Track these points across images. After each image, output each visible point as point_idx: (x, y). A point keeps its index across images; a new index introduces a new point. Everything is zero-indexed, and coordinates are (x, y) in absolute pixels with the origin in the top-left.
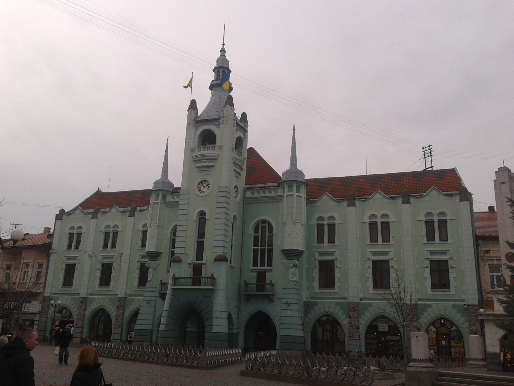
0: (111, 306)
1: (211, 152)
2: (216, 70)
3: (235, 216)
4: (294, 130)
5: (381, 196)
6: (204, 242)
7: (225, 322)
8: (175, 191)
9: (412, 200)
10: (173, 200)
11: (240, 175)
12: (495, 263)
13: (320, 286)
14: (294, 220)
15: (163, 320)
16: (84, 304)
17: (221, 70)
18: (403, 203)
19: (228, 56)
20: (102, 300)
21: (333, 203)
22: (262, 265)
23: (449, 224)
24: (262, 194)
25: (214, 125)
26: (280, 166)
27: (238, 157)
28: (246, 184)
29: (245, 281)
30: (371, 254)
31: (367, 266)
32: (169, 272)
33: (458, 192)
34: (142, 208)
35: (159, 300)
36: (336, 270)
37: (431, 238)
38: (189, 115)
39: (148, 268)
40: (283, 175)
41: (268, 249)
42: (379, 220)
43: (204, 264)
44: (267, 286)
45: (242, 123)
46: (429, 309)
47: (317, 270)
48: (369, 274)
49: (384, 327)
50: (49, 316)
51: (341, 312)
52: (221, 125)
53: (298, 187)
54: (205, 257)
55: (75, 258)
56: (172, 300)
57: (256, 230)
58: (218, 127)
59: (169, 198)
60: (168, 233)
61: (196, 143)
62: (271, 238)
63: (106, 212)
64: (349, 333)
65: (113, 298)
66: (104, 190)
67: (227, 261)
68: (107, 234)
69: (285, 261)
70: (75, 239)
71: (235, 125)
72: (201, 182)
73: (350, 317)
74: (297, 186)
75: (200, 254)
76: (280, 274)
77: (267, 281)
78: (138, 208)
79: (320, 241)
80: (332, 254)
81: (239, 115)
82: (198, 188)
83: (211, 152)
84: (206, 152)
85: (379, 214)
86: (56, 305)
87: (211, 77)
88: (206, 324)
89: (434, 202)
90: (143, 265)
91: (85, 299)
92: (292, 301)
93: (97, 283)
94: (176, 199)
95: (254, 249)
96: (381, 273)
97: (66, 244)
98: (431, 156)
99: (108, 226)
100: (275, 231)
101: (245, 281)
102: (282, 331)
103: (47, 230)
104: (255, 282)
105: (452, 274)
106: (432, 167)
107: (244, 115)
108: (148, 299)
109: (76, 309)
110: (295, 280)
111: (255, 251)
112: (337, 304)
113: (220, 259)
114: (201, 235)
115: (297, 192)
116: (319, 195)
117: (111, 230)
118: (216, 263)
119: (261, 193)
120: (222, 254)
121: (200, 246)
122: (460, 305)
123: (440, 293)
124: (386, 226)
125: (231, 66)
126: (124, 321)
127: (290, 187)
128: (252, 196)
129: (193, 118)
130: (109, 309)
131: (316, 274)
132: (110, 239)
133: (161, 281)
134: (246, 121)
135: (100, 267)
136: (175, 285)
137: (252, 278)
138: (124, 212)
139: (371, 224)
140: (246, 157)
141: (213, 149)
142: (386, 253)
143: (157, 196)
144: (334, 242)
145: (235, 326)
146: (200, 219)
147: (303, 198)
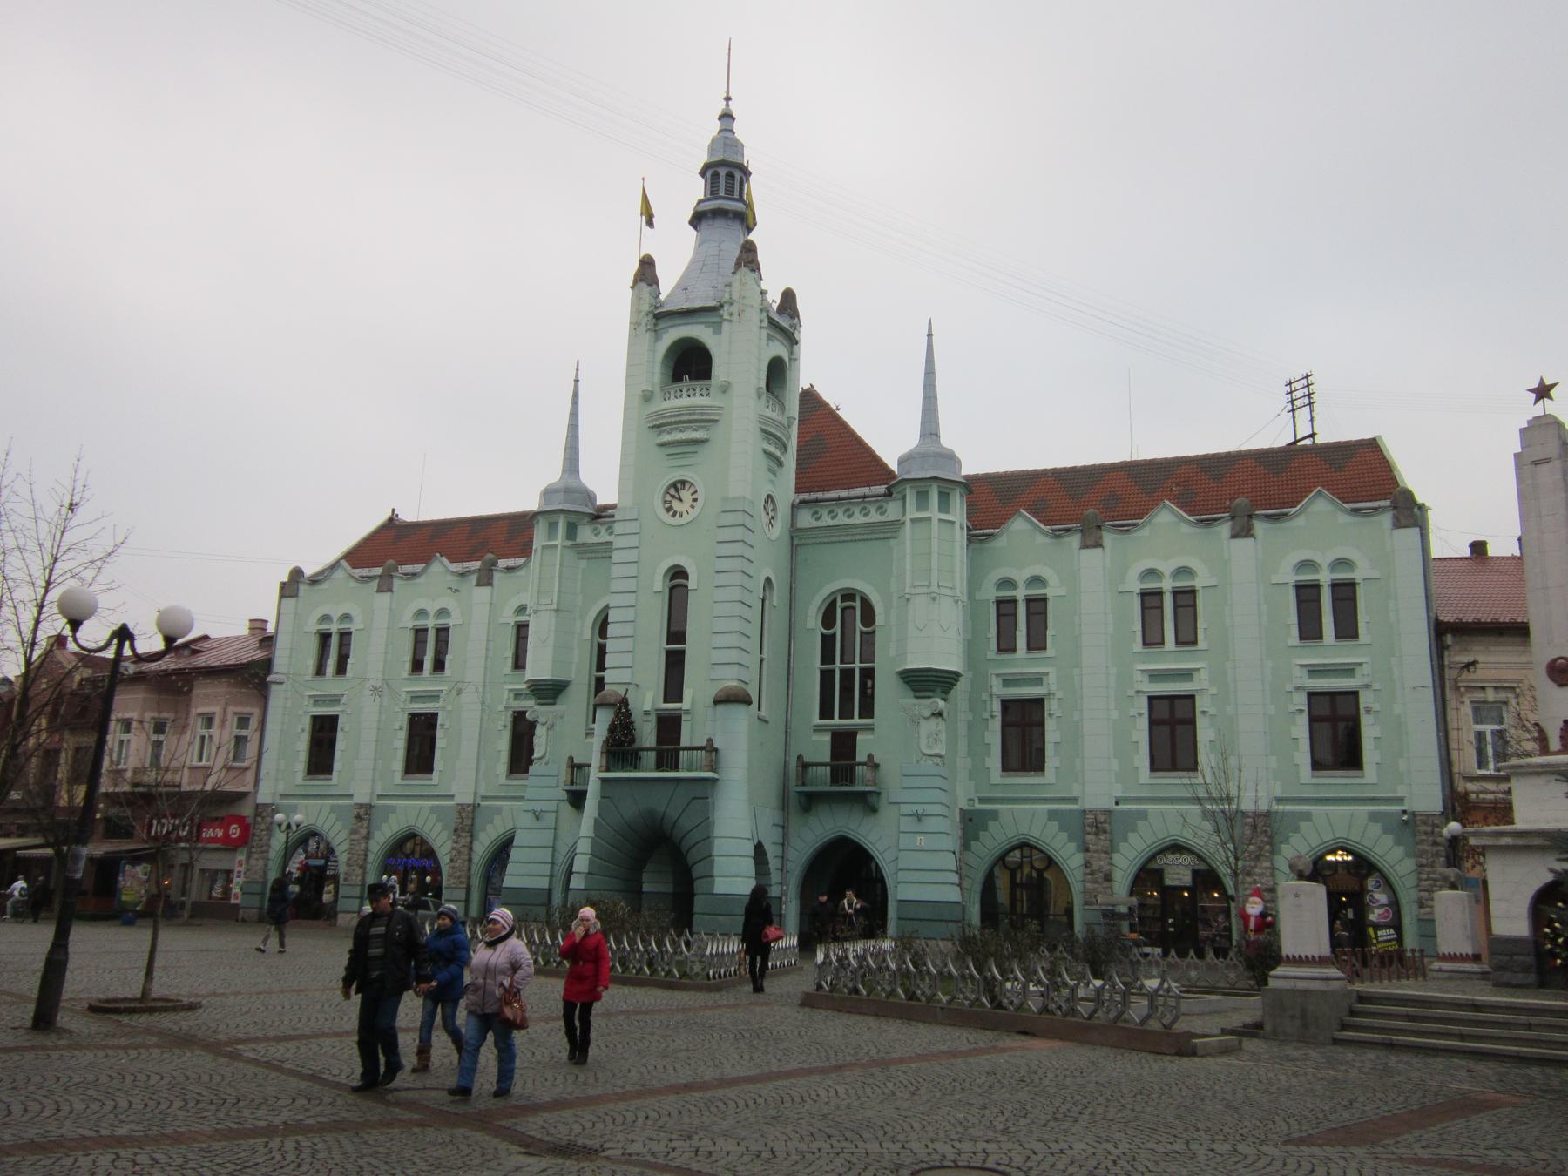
0: (439, 826)
2: (711, 171)
3: (768, 580)
4: (930, 335)
5: (1174, 519)
6: (682, 652)
7: (749, 866)
8: (601, 515)
9: (1259, 527)
10: (595, 540)
11: (780, 464)
12: (1491, 696)
13: (1006, 767)
14: (934, 588)
15: (581, 864)
16: (365, 823)
17: (723, 172)
18: (1234, 536)
19: (740, 130)
20: (416, 811)
21: (1041, 539)
22: (846, 713)
23: (1360, 591)
24: (842, 519)
25: (707, 324)
26: (890, 438)
27: (774, 415)
28: (798, 491)
29: (800, 757)
30: (1146, 678)
31: (1133, 712)
32: (590, 734)
33: (1387, 503)
34: (511, 562)
35: (567, 809)
36: (1050, 725)
37: (1309, 630)
38: (637, 300)
39: (533, 725)
40: (901, 462)
41: (861, 670)
42: (1167, 585)
43: (687, 712)
44: (859, 769)
45: (784, 319)
46: (1303, 825)
47: (996, 725)
48: (1140, 732)
49: (1179, 873)
50: (272, 854)
51: (1064, 836)
52: (725, 326)
53: (944, 497)
54: (687, 693)
55: (336, 700)
56: (601, 809)
57: (828, 620)
58: (718, 328)
59: (586, 534)
60: (586, 629)
61: (657, 378)
62: (869, 639)
63: (414, 575)
64: (1085, 891)
65: (443, 807)
66: (408, 515)
67: (749, 703)
68: (420, 633)
69: (909, 700)
70: (334, 649)
71: (765, 323)
72: (674, 485)
73: (1087, 850)
74: (940, 493)
75: (673, 688)
76: (896, 737)
77: (861, 756)
78: (502, 563)
79: (1006, 644)
80: (1037, 680)
81: (774, 298)
83: (698, 400)
84: (684, 401)
85: (1167, 568)
86: (289, 826)
87: (697, 189)
88: (697, 871)
89: (1322, 534)
90: (519, 717)
91: (368, 807)
92: (930, 809)
93: (399, 765)
94: (604, 537)
95: (823, 672)
96: (1172, 730)
97: (311, 663)
98: (1310, 404)
99: (422, 613)
100: (879, 620)
101: (800, 757)
102: (903, 889)
103: (258, 625)
104: (828, 760)
105: (1369, 731)
106: (1312, 436)
107: (789, 298)
108: (538, 806)
109: (343, 835)
110: (936, 751)
111: (827, 677)
112: (1053, 815)
113: (732, 698)
114: (676, 635)
115: (940, 511)
116: (999, 522)
117: (431, 623)
118: (720, 708)
119: (840, 514)
120: (735, 683)
121: (675, 663)
122: (1386, 814)
123: (1338, 781)
124: (1186, 599)
125: (750, 158)
126: (473, 867)
127: (922, 497)
128: (815, 524)
129: (646, 308)
130: (433, 835)
131: (993, 736)
132: (430, 648)
133: (571, 758)
134: (794, 314)
135: (405, 724)
136: (608, 770)
137: (819, 748)
138: (462, 575)
139: (1144, 595)
140: (796, 414)
142: (1187, 675)
143: (553, 526)
144: (1042, 647)
145: (775, 877)
146: (671, 589)
147: (957, 526)
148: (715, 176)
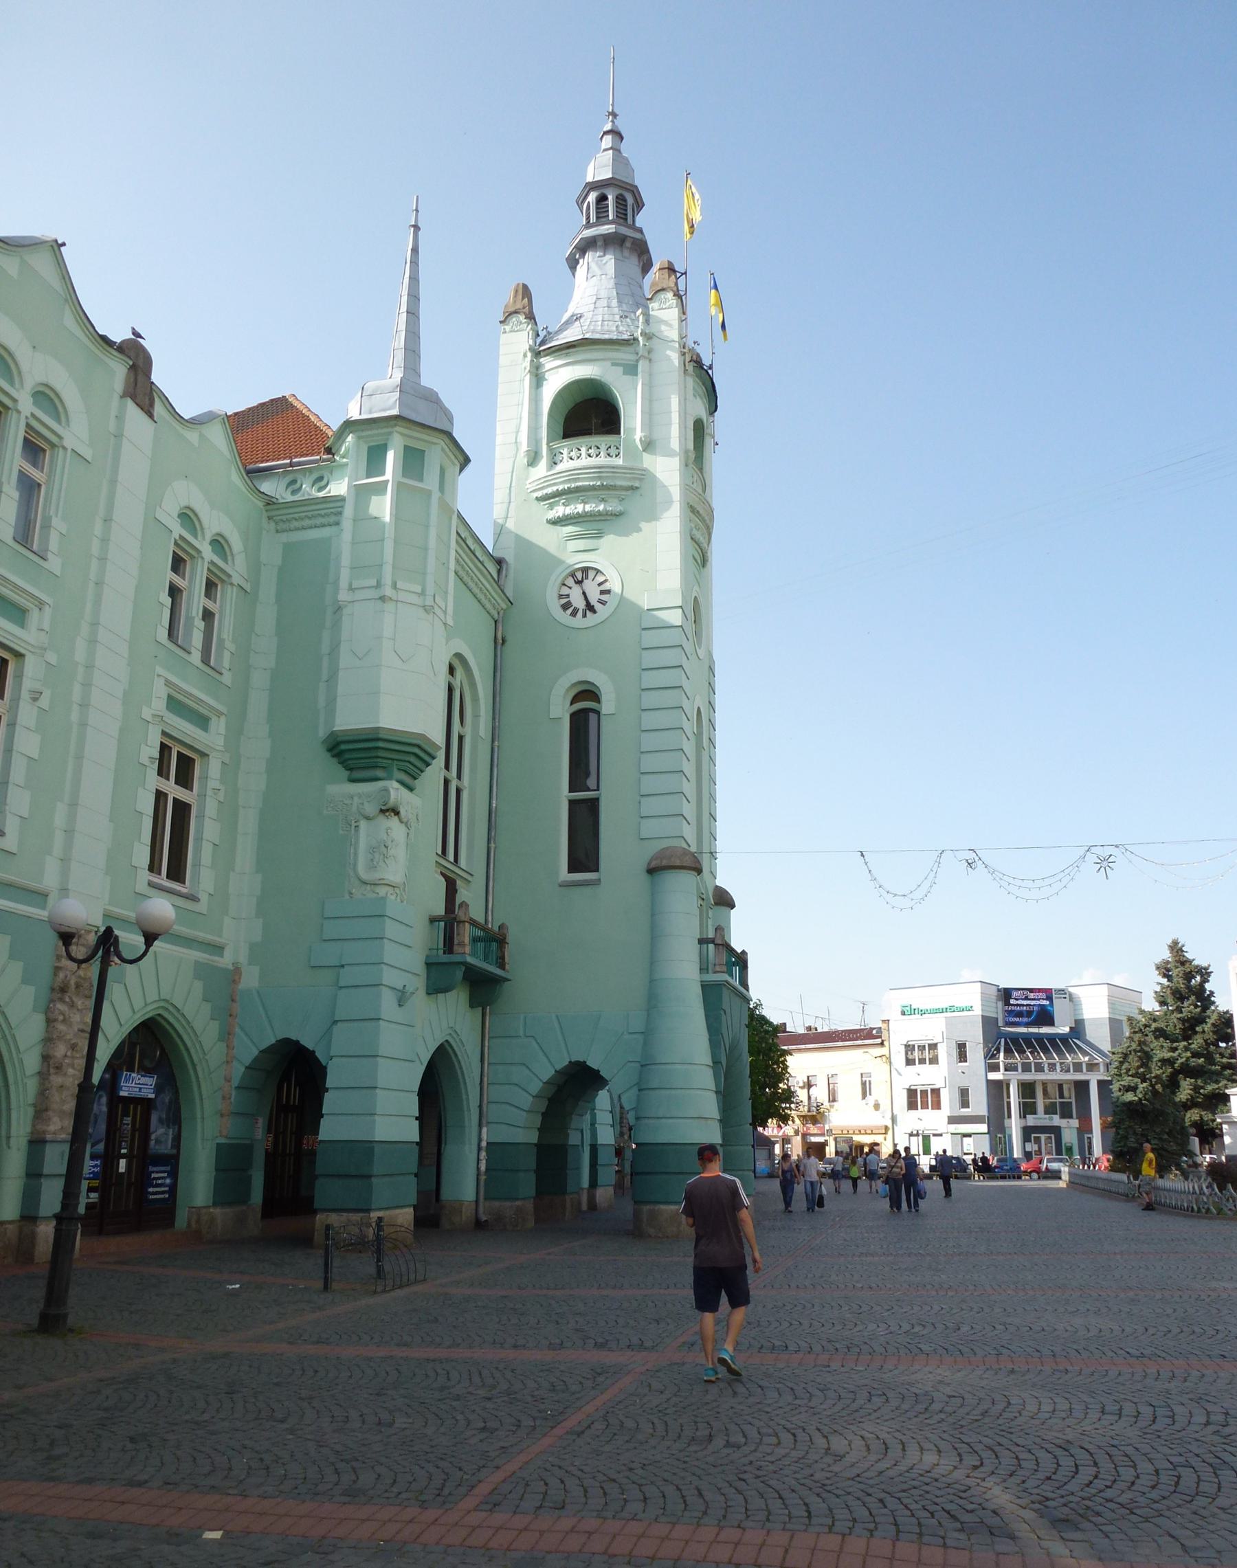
1: (602, 460)
6: (597, 800)
72: (573, 575)
82: (561, 597)
141: (613, 451)
148: (602, 199)
